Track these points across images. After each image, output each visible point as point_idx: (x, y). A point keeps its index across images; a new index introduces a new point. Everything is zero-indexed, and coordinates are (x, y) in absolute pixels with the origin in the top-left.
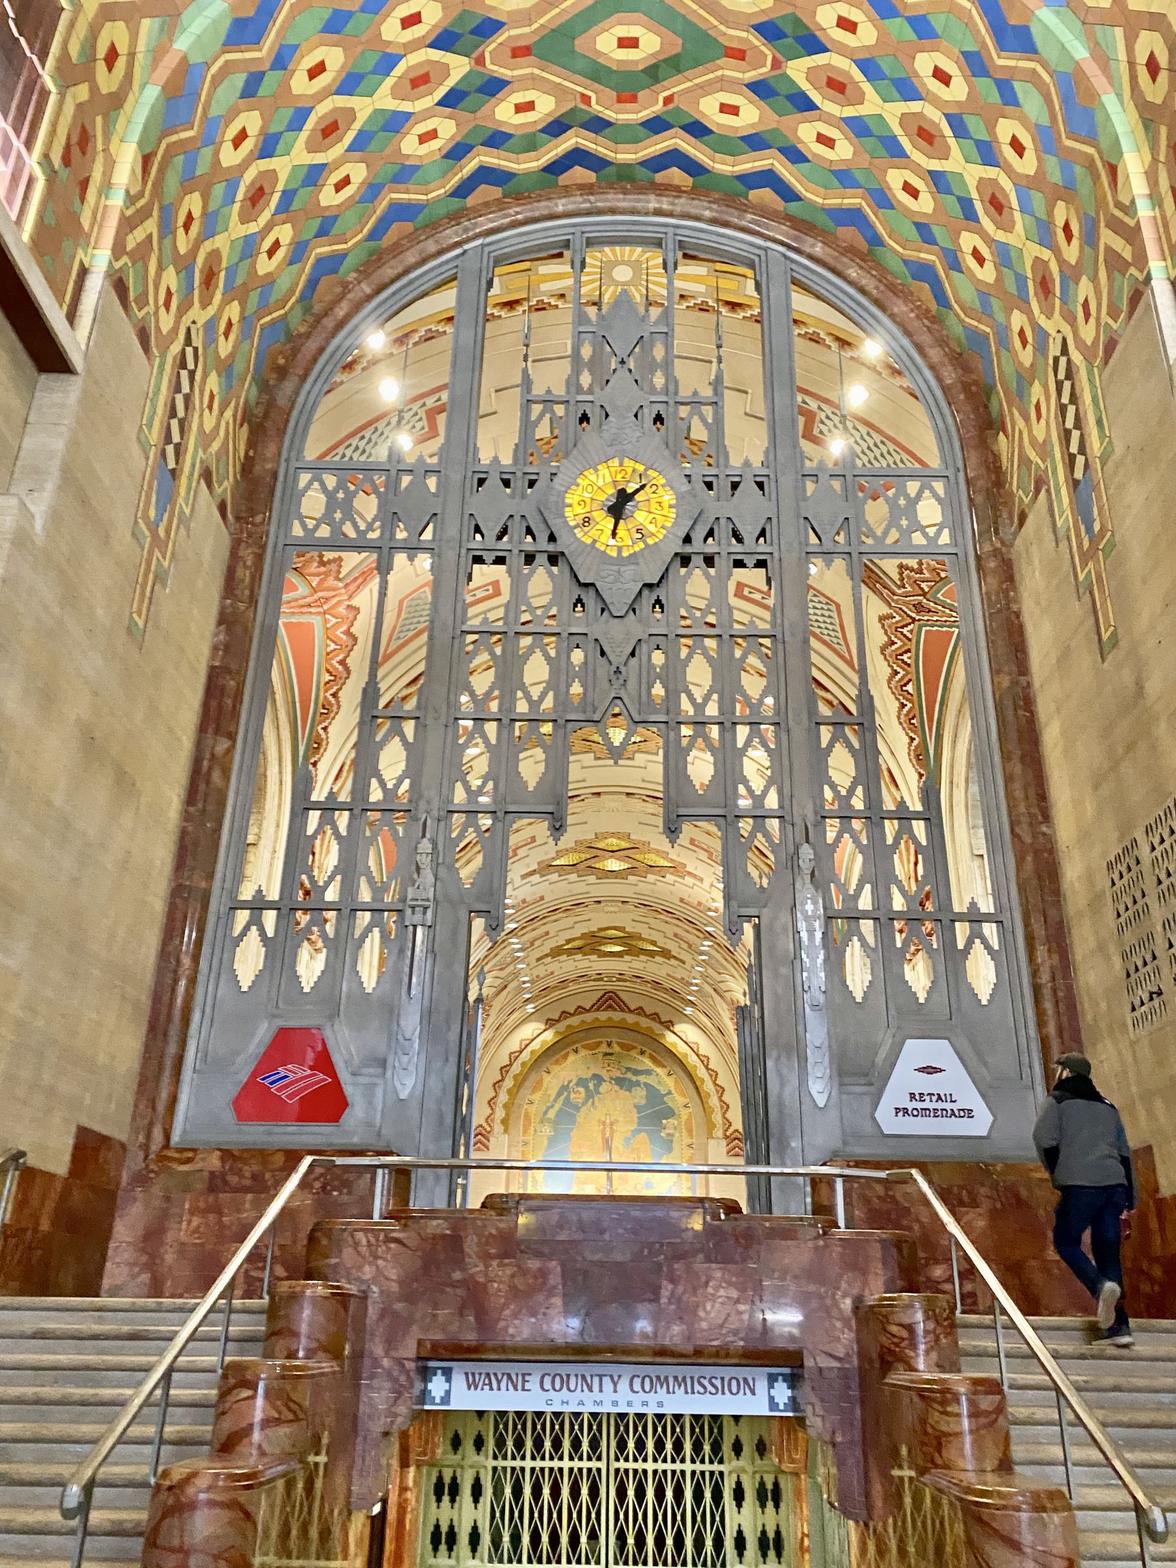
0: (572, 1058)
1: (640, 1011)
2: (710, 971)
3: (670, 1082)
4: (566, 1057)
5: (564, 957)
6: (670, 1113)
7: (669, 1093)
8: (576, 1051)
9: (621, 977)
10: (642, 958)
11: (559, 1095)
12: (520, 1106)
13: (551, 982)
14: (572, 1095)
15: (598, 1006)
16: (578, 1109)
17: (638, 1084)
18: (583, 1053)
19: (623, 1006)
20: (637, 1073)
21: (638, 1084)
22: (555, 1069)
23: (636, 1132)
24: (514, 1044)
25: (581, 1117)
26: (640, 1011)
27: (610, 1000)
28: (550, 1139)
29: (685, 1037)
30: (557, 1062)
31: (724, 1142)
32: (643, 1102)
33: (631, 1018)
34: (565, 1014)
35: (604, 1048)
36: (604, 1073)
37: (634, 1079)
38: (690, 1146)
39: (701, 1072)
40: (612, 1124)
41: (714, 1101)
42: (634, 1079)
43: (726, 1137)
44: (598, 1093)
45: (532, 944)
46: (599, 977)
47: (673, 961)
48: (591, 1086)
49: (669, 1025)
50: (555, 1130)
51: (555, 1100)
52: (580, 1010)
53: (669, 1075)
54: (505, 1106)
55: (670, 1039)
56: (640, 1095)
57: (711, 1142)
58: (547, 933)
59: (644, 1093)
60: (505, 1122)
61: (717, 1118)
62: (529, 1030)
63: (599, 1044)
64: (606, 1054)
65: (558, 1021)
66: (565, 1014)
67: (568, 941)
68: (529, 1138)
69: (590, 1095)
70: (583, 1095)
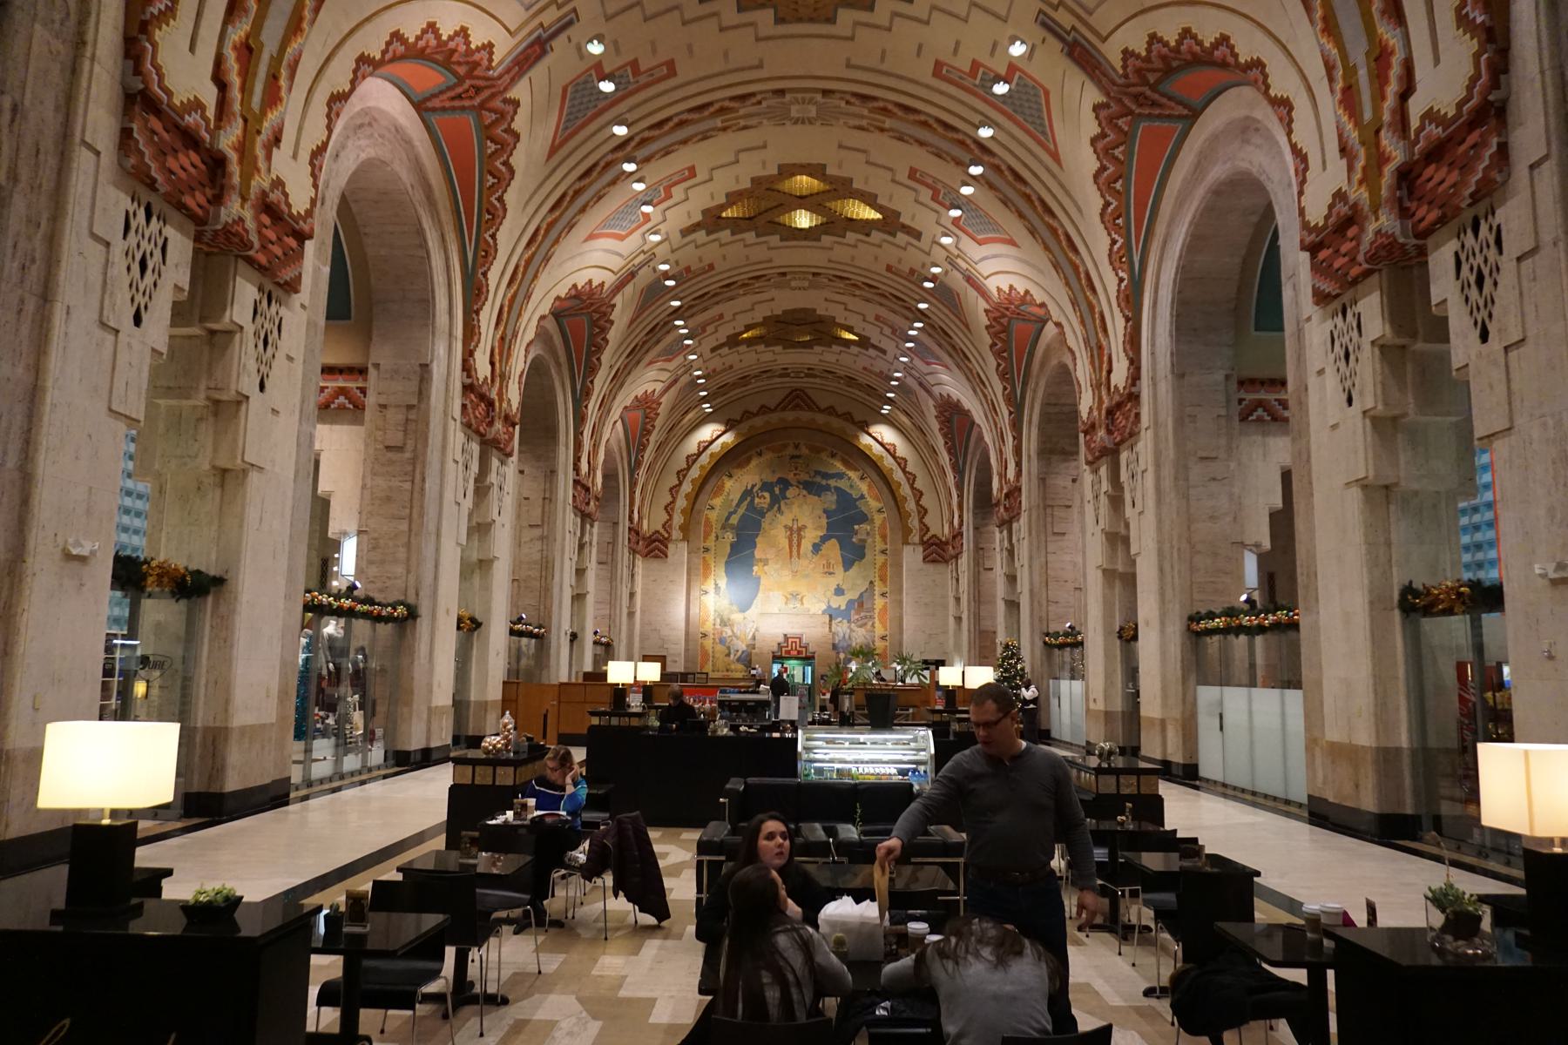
0: (754, 463)
1: (831, 411)
2: (918, 362)
3: (864, 487)
4: (748, 461)
5: (743, 348)
6: (863, 518)
7: (862, 497)
8: (760, 454)
9: (810, 373)
12: (700, 511)
15: (782, 406)
16: (763, 515)
17: (828, 488)
18: (768, 456)
19: (811, 406)
20: (827, 476)
21: (828, 488)
22: (738, 473)
23: (824, 539)
24: (692, 444)
25: (765, 524)
26: (831, 411)
27: (797, 399)
28: (732, 546)
29: (882, 437)
30: (740, 466)
33: (821, 419)
34: (747, 415)
35: (790, 451)
36: (790, 477)
38: (883, 552)
39: (898, 475)
40: (799, 530)
41: (911, 505)
43: (922, 543)
45: (704, 330)
46: (785, 373)
47: (872, 352)
48: (777, 490)
49: (864, 426)
51: (738, 505)
52: (764, 409)
54: (683, 512)
55: (865, 440)
56: (830, 499)
58: (721, 316)
60: (685, 529)
61: (914, 523)
62: (707, 432)
63: (785, 446)
64: (793, 457)
65: (740, 422)
66: (747, 415)
68: (711, 543)
69: (775, 501)
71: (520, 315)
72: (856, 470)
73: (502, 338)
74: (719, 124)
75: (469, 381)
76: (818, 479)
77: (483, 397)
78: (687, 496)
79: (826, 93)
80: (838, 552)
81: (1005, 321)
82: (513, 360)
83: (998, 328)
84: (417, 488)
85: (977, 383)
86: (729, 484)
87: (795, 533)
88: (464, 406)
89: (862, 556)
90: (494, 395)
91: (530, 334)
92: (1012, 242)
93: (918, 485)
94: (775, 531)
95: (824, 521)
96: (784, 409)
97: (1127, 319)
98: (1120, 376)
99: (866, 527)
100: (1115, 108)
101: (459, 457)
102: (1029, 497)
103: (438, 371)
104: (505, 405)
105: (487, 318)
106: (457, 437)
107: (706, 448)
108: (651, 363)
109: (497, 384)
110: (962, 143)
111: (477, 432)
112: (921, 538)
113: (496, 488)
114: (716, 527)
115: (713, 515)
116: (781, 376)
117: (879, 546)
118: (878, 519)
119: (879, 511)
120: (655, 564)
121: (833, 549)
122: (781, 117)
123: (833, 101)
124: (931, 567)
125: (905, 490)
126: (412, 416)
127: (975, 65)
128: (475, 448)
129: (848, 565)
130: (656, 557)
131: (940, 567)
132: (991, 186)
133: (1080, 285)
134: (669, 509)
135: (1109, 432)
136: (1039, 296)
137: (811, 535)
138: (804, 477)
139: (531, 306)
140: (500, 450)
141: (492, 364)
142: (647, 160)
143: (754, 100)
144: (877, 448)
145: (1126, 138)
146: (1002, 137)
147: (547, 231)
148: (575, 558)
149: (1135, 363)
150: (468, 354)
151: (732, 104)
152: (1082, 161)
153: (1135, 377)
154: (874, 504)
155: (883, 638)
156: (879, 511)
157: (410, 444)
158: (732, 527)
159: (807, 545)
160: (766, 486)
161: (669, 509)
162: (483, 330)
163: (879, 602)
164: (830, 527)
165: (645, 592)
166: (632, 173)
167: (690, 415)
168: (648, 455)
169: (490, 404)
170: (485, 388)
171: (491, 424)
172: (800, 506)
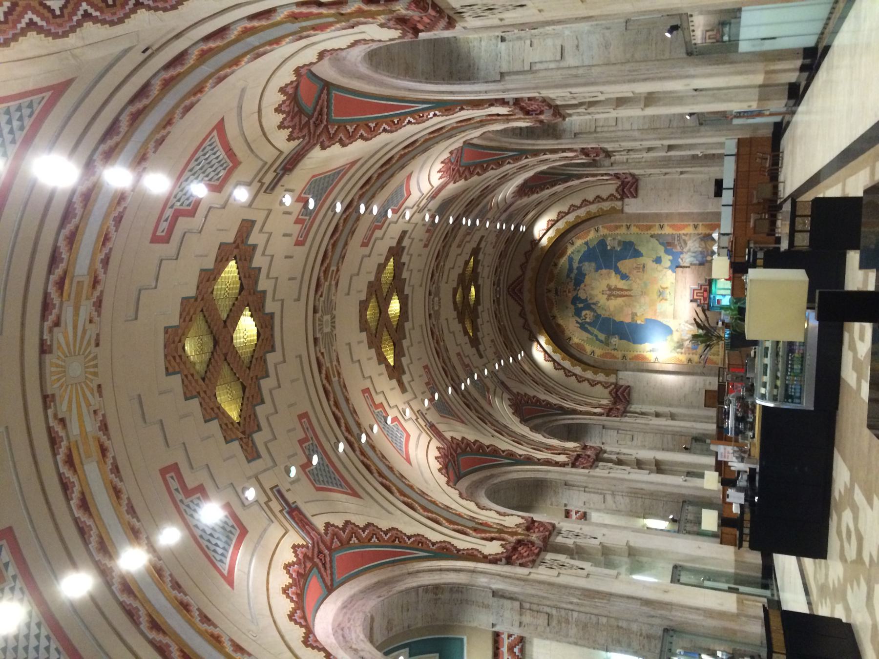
0: (561, 322)
1: (523, 267)
2: (489, 215)
3: (579, 243)
4: (559, 326)
5: (480, 334)
6: (602, 243)
7: (586, 243)
8: (554, 317)
9: (496, 284)
10: (479, 270)
11: (586, 330)
12: (595, 361)
13: (500, 340)
14: (588, 320)
15: (519, 301)
16: (598, 316)
17: (579, 269)
18: (555, 311)
19: (519, 281)
20: (571, 269)
21: (579, 269)
22: (568, 333)
23: (617, 271)
25: (604, 314)
26: (523, 267)
27: (515, 290)
28: (621, 339)
29: (543, 230)
30: (563, 332)
31: (626, 200)
32: (593, 264)
33: (529, 274)
34: (526, 326)
35: (552, 295)
37: (575, 271)
38: (628, 227)
39: (571, 218)
41: (593, 208)
42: (575, 271)
43: (622, 199)
44: (586, 300)
45: (468, 366)
46: (497, 301)
47: (482, 245)
48: (581, 305)
49: (535, 243)
50: (614, 334)
51: (591, 333)
52: (522, 314)
53: (573, 244)
54: (595, 373)
55: (544, 242)
56: (588, 267)
57: (627, 209)
58: (458, 354)
59: (586, 263)
60: (608, 371)
61: (606, 206)
62: (538, 355)
64: (556, 293)
66: (526, 326)
67: (466, 333)
68: (619, 354)
69: (588, 307)
70: (587, 312)
71: (459, 515)
72: (566, 248)
73: (475, 530)
74: (337, 378)
75: (504, 560)
76: (573, 276)
77: (515, 549)
78: (584, 370)
79: (315, 311)
80: (627, 261)
81: (461, 170)
82: (490, 521)
83: (467, 173)
84: (577, 608)
85: (504, 179)
86: (576, 340)
87: (613, 293)
88: (521, 565)
89: (631, 244)
90: (513, 539)
91: (472, 505)
92: (409, 177)
93: (578, 202)
94: (611, 306)
95: (604, 271)
96: (523, 301)
97: (462, 109)
98: (503, 110)
99: (609, 241)
100: (324, 138)
101: (555, 572)
102: (588, 143)
103: (498, 585)
104: (520, 530)
105: (463, 543)
106: (541, 573)
107: (549, 356)
108: (490, 404)
109: (506, 536)
110: (345, 220)
111: (538, 554)
112: (617, 199)
113: (579, 541)
114: (608, 350)
115: (598, 352)
116: (499, 305)
117: (623, 230)
118: (603, 231)
119: (597, 231)
120: (635, 396)
121: (625, 265)
122: (331, 337)
123: (320, 305)
124: (641, 192)
125: (582, 213)
126: (527, 606)
127: (297, 221)
128: (549, 556)
129: (637, 254)
130: (629, 394)
131: (641, 184)
132: (373, 196)
133: (438, 135)
134: (593, 383)
135: (541, 113)
136: (446, 155)
137: (614, 281)
138: (571, 286)
139: (454, 506)
140: (550, 534)
141: (492, 539)
142: (359, 425)
143: (321, 357)
144: (551, 233)
145: (342, 126)
146: (341, 197)
147: (404, 495)
148: (628, 468)
149: (492, 103)
150: (486, 559)
151: (324, 372)
152: (358, 148)
153: (503, 102)
154: (592, 235)
155: (696, 227)
156: (597, 231)
157: (548, 610)
158: (607, 339)
159: (622, 284)
160: (578, 313)
161: (593, 383)
162: (470, 546)
163: (667, 230)
164: (608, 267)
165: (656, 403)
166: (367, 435)
167: (526, 368)
168: (554, 400)
169: (519, 542)
170: (509, 547)
171: (533, 543)
172: (592, 289)
